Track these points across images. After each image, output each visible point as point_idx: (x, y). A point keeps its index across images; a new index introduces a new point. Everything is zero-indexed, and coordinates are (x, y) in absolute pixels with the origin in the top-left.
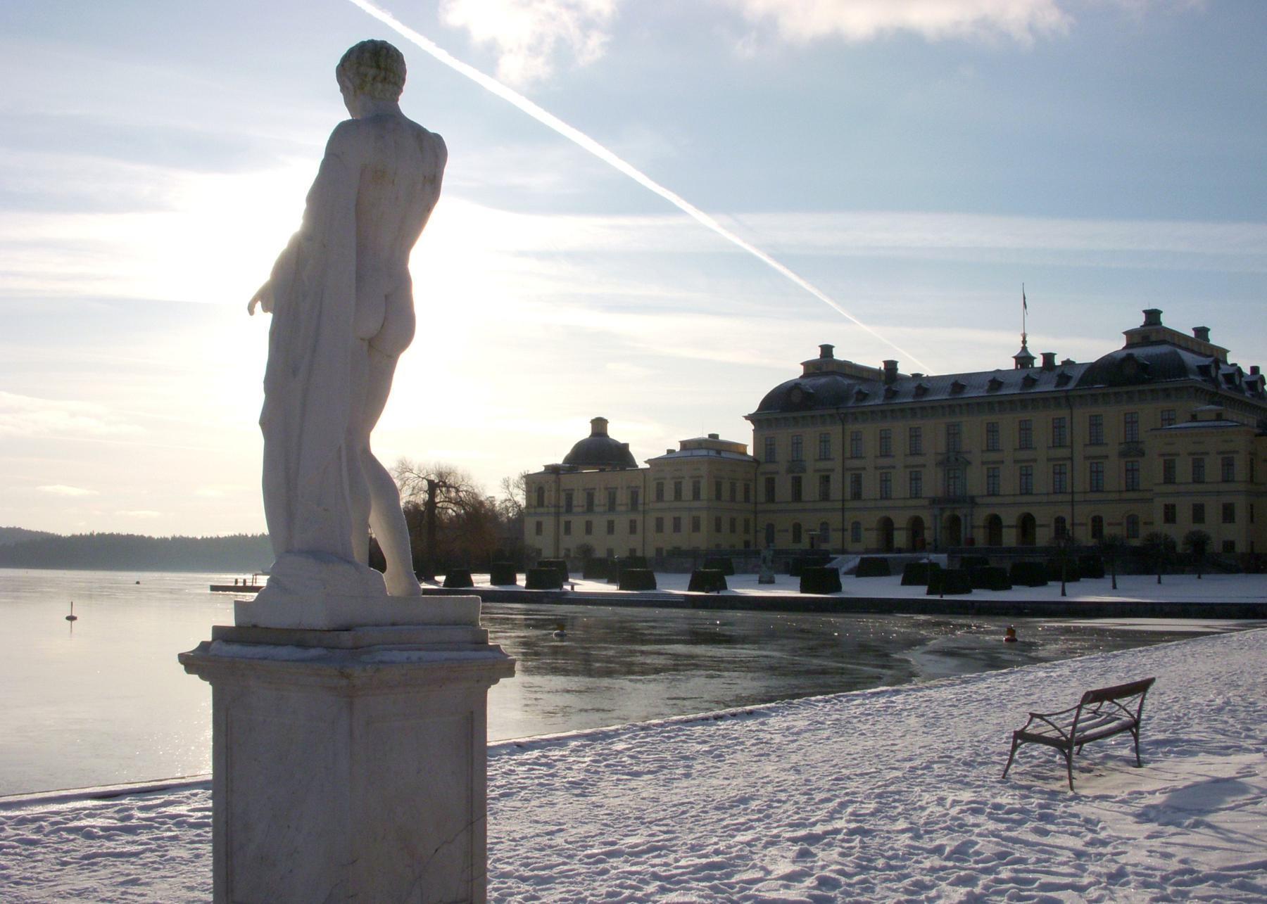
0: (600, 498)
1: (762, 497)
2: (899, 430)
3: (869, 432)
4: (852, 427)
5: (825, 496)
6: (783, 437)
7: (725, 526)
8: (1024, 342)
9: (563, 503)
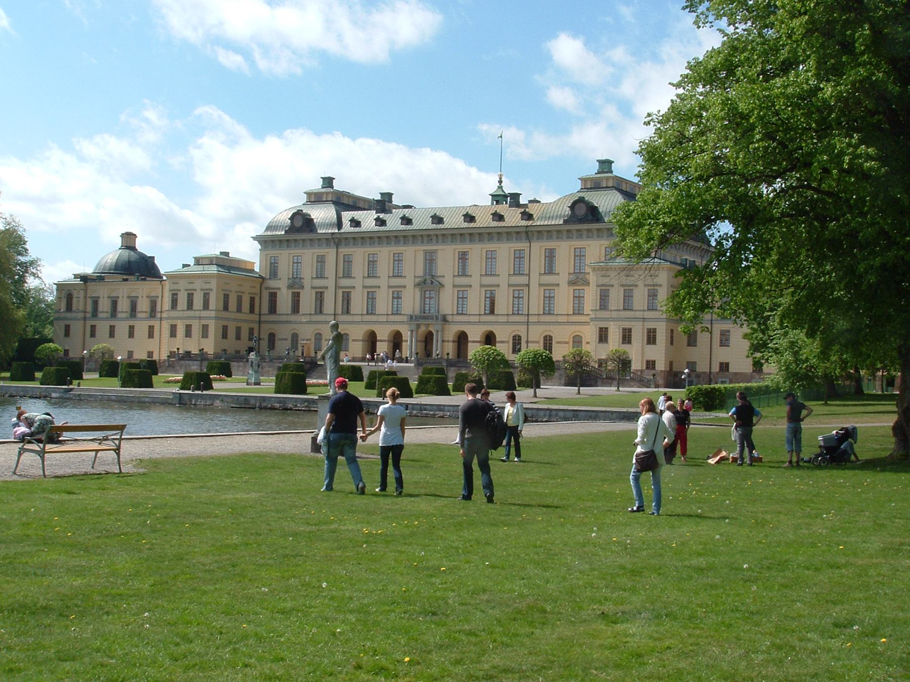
0: (124, 306)
1: (265, 308)
3: (359, 255)
4: (344, 250)
5: (320, 310)
6: (285, 257)
7: (231, 333)
8: (500, 182)
9: (89, 308)
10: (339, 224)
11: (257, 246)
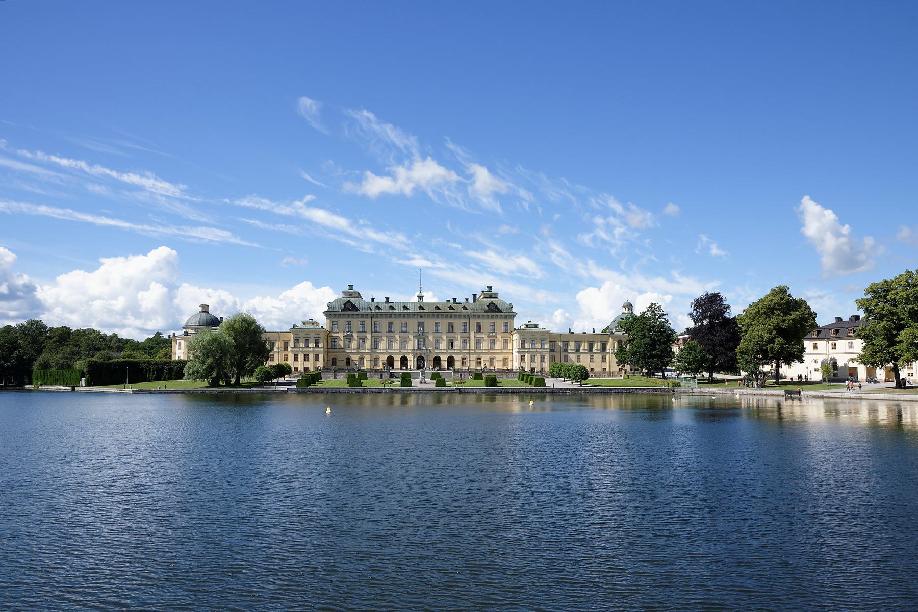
4: (374, 320)
6: (342, 322)
11: (324, 317)
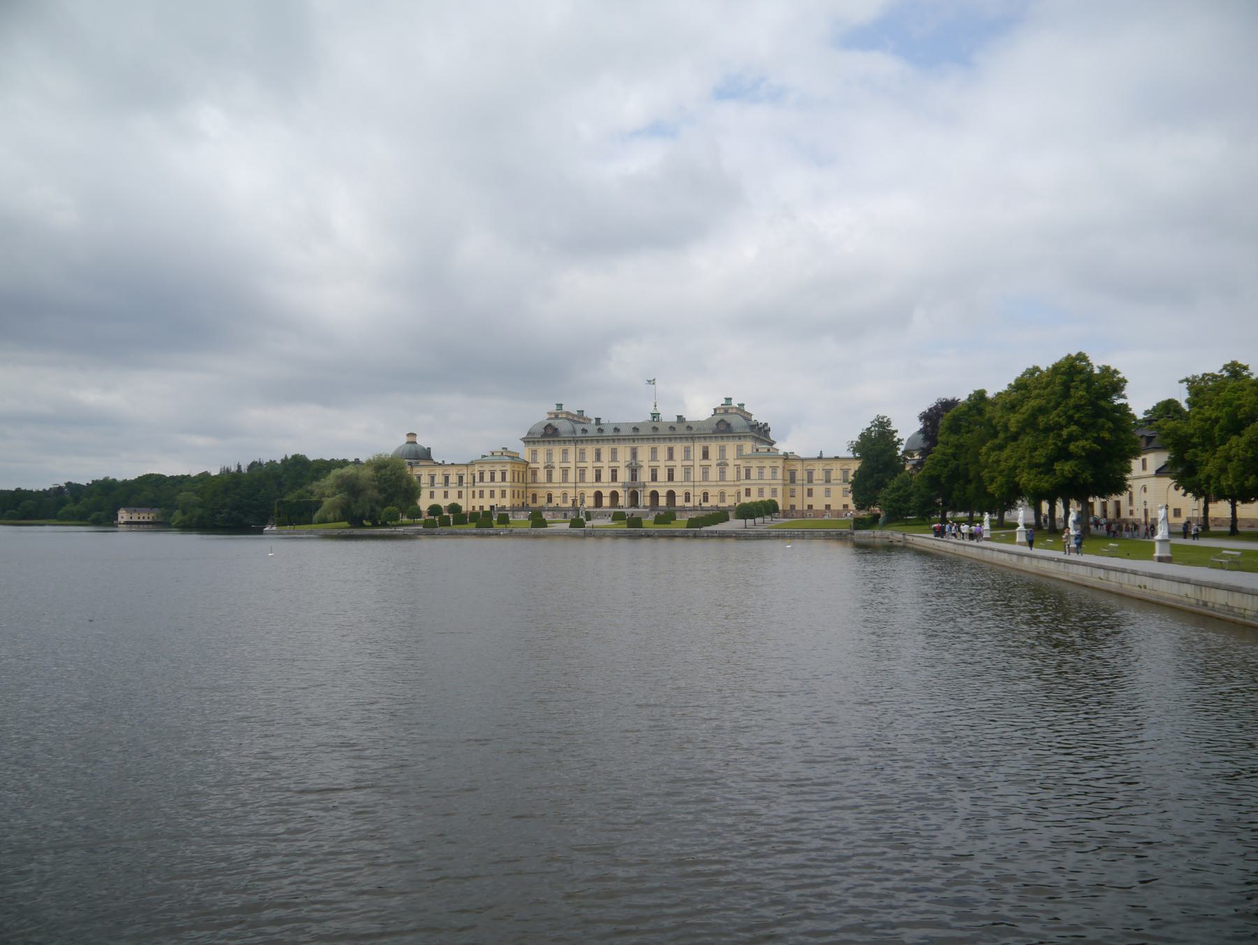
0: (439, 479)
1: (529, 480)
2: (606, 450)
3: (590, 450)
4: (580, 446)
6: (542, 451)
10: (575, 432)
